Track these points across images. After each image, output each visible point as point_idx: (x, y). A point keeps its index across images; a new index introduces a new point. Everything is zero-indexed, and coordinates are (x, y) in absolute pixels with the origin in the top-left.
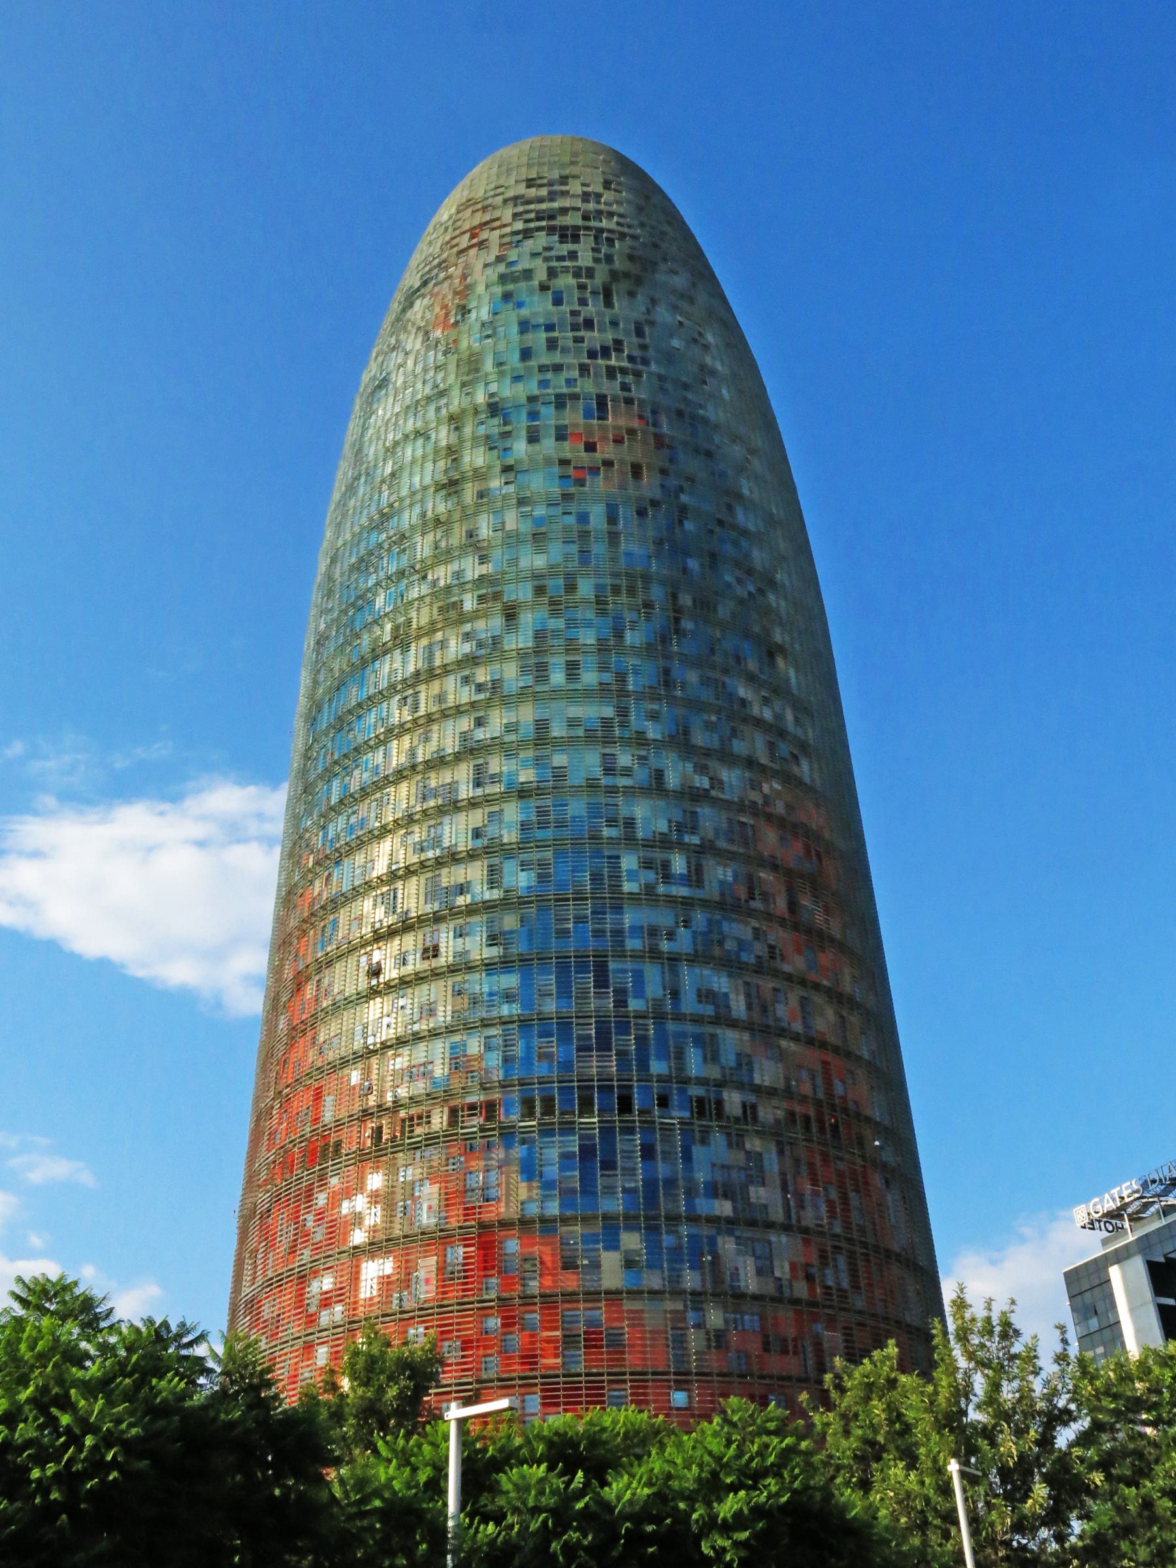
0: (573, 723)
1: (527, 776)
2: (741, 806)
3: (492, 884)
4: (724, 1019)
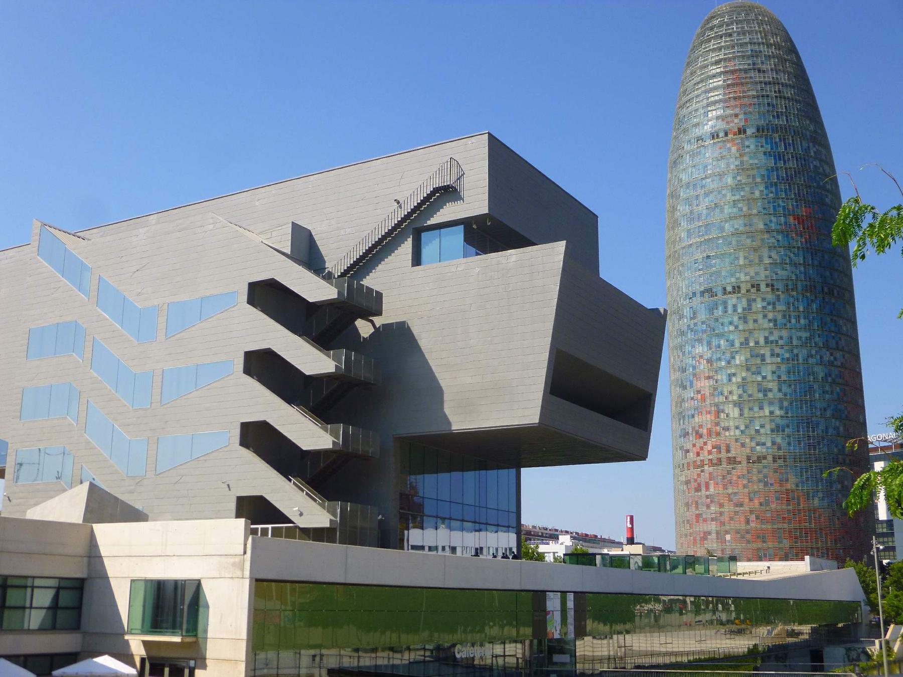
0: (800, 338)
1: (787, 355)
2: (842, 366)
3: (780, 390)
4: (838, 434)
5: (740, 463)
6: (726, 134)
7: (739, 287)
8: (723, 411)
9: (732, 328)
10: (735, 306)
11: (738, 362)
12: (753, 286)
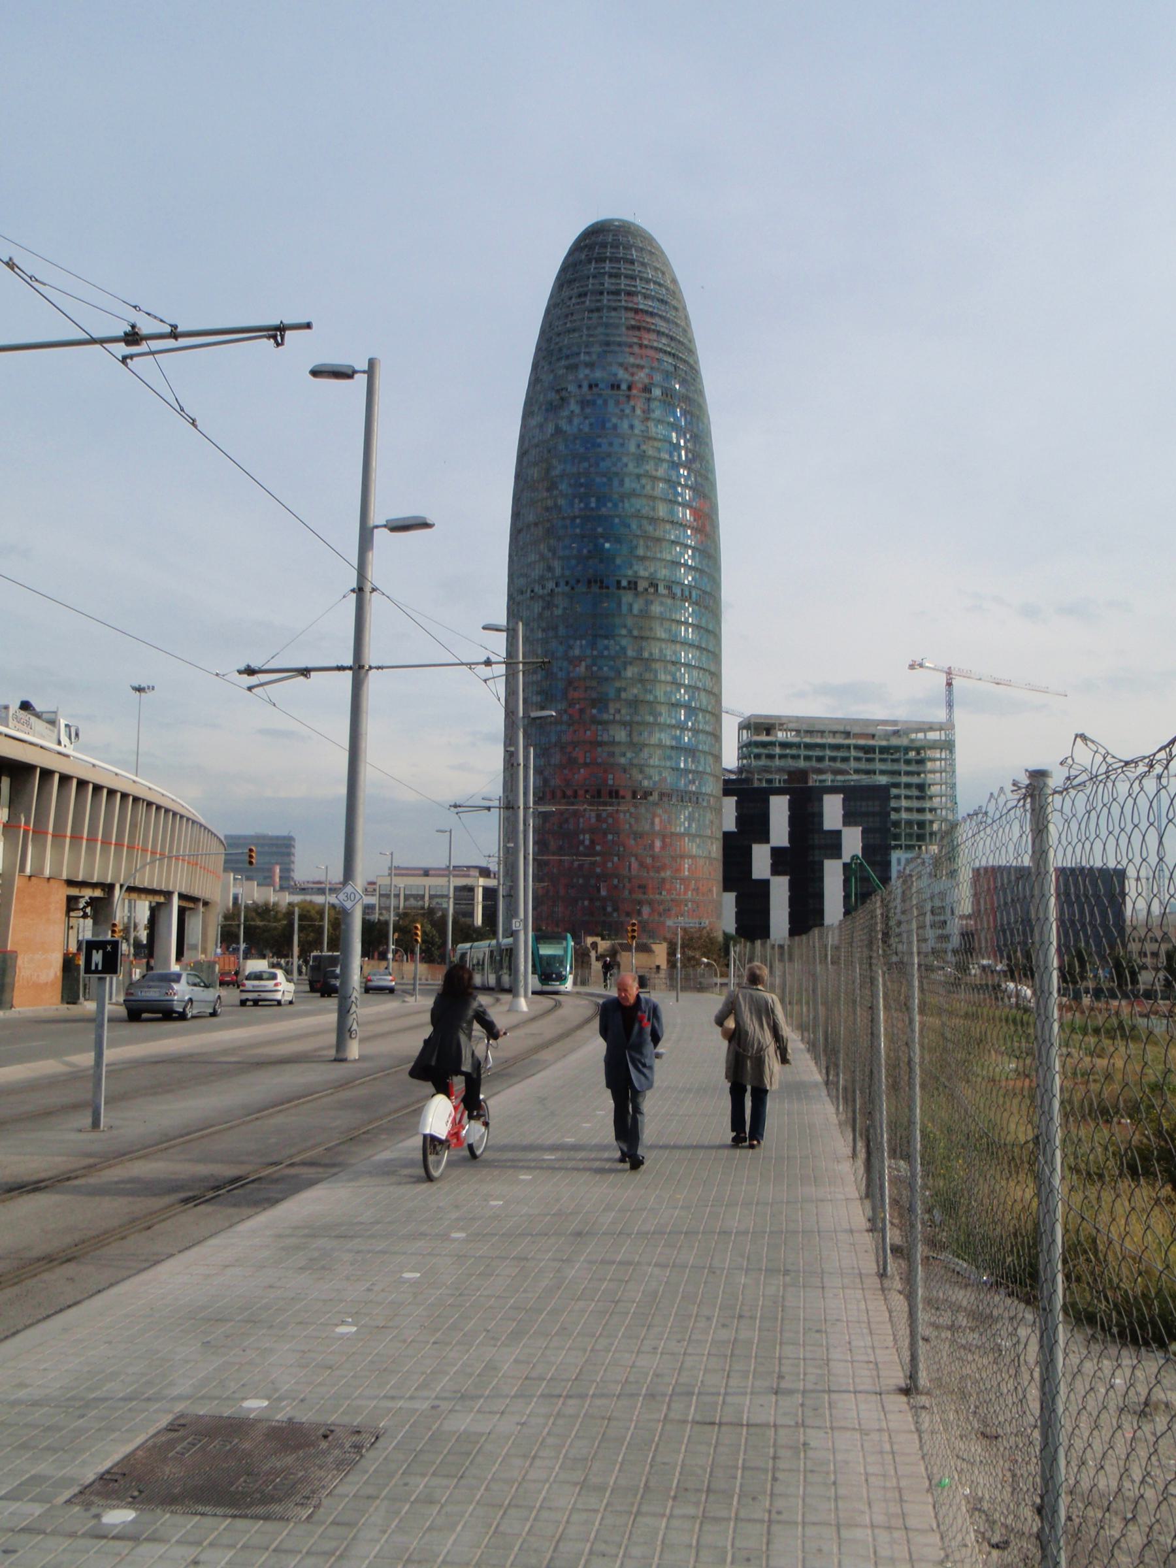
5: (623, 797)
6: (630, 388)
7: (636, 583)
9: (624, 632)
10: (631, 606)
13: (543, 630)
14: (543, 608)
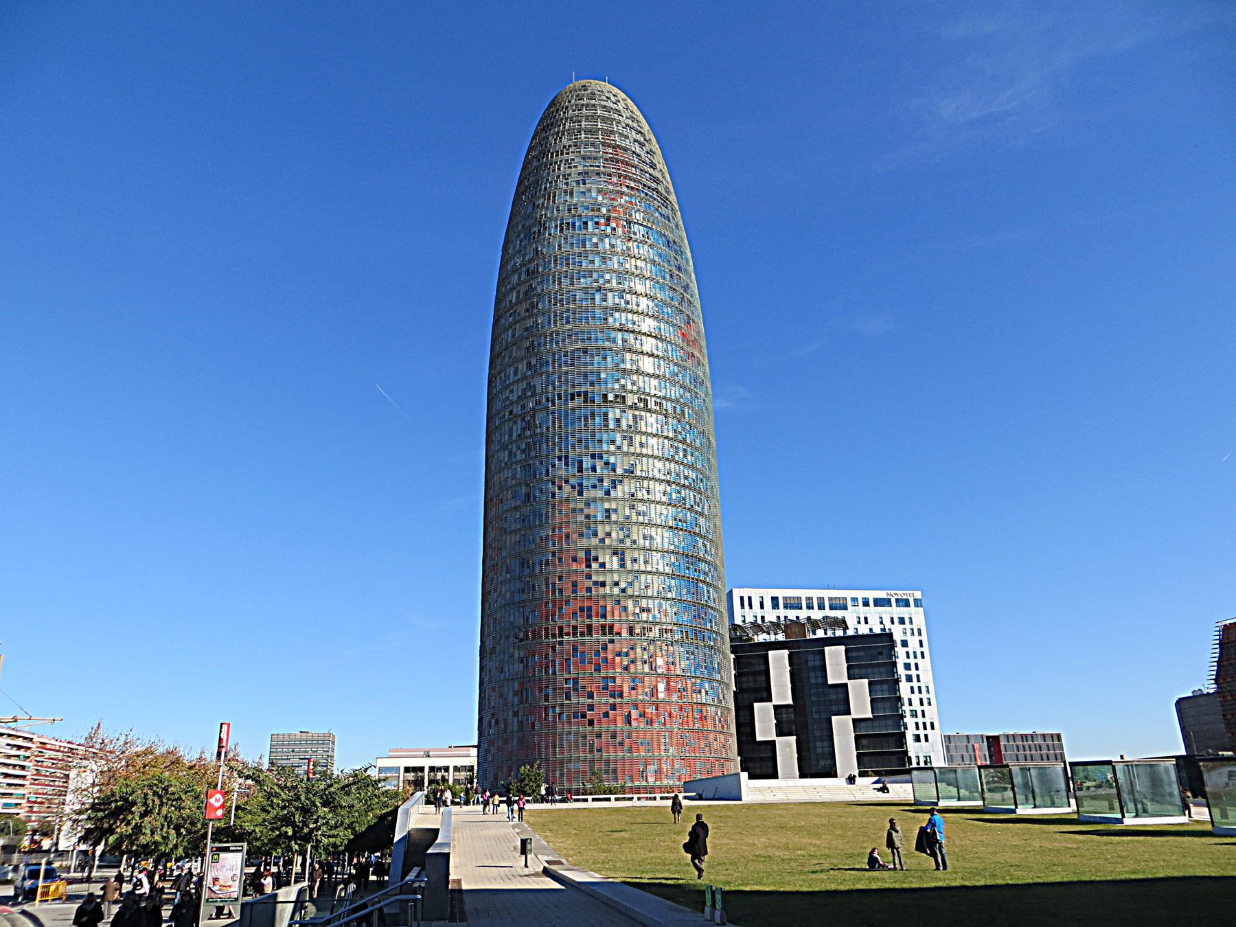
6: (609, 211)
8: (596, 559)
9: (612, 448)
10: (618, 421)
11: (620, 495)
12: (640, 400)
13: (524, 451)
14: (524, 429)
